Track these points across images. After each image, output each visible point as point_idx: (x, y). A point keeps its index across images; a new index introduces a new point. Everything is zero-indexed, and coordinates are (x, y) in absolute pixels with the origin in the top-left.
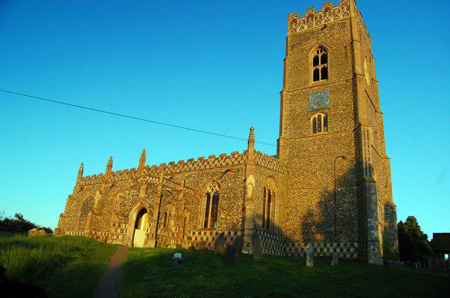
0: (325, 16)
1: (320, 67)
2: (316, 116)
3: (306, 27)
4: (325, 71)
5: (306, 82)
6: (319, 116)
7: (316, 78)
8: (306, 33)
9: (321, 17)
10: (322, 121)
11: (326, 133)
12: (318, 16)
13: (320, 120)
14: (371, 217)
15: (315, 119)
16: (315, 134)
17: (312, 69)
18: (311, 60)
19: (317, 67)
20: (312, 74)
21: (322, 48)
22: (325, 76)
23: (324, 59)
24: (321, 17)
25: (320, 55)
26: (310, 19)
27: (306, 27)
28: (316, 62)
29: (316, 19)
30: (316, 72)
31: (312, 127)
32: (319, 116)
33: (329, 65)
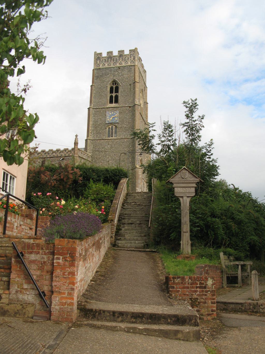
0: (119, 60)
1: (114, 95)
2: (110, 127)
3: (106, 65)
4: (117, 97)
7: (111, 102)
10: (114, 131)
12: (115, 59)
13: (112, 129)
17: (109, 95)
18: (109, 89)
19: (112, 94)
22: (116, 101)
24: (116, 60)
25: (114, 87)
27: (106, 65)
28: (111, 91)
29: (113, 60)
30: (111, 97)
33: (119, 94)
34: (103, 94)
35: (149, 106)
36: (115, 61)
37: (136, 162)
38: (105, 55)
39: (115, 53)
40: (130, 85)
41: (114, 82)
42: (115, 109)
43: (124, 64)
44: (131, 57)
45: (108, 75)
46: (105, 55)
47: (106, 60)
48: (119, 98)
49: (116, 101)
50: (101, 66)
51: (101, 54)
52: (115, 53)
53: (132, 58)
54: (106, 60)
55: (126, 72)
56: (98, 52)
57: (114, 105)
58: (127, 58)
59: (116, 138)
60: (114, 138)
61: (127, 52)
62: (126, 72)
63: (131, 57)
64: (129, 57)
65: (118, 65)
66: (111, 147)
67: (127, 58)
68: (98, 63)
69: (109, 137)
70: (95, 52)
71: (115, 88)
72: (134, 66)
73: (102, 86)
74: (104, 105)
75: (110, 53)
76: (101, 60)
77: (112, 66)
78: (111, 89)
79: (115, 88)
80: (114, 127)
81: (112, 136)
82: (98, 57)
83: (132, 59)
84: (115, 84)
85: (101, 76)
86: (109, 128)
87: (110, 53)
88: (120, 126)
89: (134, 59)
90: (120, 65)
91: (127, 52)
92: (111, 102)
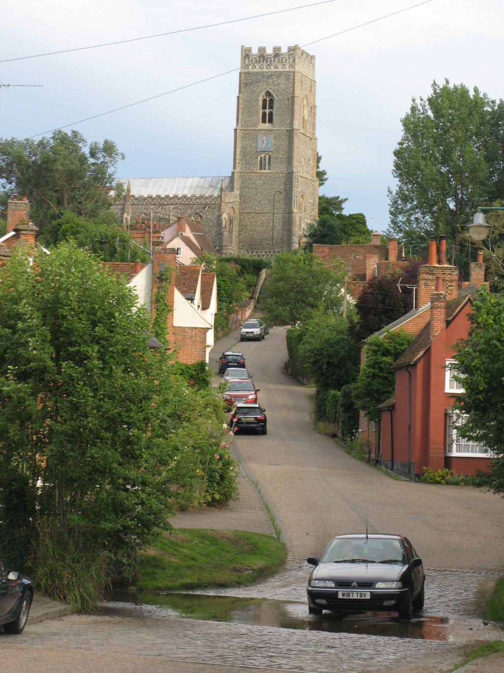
1: (267, 111)
2: (263, 156)
3: (257, 67)
4: (271, 114)
5: (256, 125)
6: (265, 156)
7: (264, 121)
8: (258, 73)
9: (271, 61)
10: (267, 161)
11: (269, 171)
13: (265, 160)
14: (294, 236)
15: (261, 157)
16: (261, 171)
18: (261, 103)
20: (261, 116)
21: (268, 94)
22: (271, 121)
23: (271, 107)
24: (271, 61)
25: (268, 99)
26: (262, 59)
27: (257, 67)
28: (264, 107)
30: (264, 114)
31: (259, 163)
32: (265, 156)
33: (275, 111)
34: (253, 110)
35: (318, 111)
36: (269, 62)
37: (293, 204)
38: (255, 51)
39: (269, 51)
40: (288, 99)
41: (268, 94)
42: (269, 132)
43: (280, 69)
44: (289, 58)
45: (259, 82)
46: (255, 51)
47: (258, 59)
48: (274, 117)
49: (271, 121)
50: (250, 69)
51: (250, 50)
52: (269, 51)
53: (292, 59)
54: (258, 59)
55: (282, 80)
56: (247, 46)
57: (267, 126)
58: (284, 60)
59: (269, 171)
60: (267, 171)
61: (284, 50)
62: (282, 80)
63: (289, 58)
64: (287, 58)
65: (273, 69)
66: (264, 183)
67: (284, 60)
68: (247, 63)
69: (261, 169)
70: (242, 46)
71: (269, 102)
72: (294, 72)
73: (252, 99)
74: (254, 126)
75: (262, 50)
76: (251, 59)
77: (265, 70)
78: (265, 101)
79: (269, 102)
80: (267, 156)
81: (265, 169)
82: (246, 54)
83: (291, 62)
84: (269, 96)
85: (251, 84)
86: (261, 157)
87: (262, 50)
88: (275, 156)
89: (294, 61)
90: (276, 70)
91: (284, 50)
92: (264, 121)
